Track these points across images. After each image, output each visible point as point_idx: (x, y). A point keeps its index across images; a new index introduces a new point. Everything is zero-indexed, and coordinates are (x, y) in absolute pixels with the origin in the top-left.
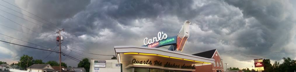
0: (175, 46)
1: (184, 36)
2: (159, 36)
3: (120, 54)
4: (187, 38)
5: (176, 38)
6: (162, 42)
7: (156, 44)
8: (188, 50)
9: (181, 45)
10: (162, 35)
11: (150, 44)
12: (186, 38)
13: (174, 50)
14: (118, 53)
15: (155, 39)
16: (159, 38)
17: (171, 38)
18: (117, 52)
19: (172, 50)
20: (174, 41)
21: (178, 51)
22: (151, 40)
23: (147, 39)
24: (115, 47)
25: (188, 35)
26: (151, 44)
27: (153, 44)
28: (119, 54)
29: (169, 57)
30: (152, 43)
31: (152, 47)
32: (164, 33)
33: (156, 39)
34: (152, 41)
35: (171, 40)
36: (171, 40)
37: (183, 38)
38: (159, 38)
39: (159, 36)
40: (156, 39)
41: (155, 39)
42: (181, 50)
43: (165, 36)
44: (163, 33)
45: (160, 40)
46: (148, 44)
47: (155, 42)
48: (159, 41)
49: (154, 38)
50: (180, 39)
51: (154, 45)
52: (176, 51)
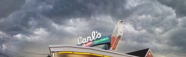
0: (109, 45)
1: (118, 36)
2: (94, 36)
3: (55, 53)
4: (121, 37)
5: (110, 37)
6: (96, 41)
7: (90, 43)
10: (96, 34)
11: (84, 43)
12: (119, 37)
13: (108, 49)
14: (52, 52)
15: (89, 38)
16: (93, 38)
17: (105, 37)
18: (51, 51)
19: (106, 49)
20: (107, 40)
21: (111, 50)
22: (85, 39)
23: (81, 38)
24: (50, 46)
25: (122, 34)
28: (53, 53)
29: (103, 56)
30: (87, 42)
31: (86, 46)
32: (98, 32)
33: (90, 39)
34: (87, 40)
35: (105, 39)
36: (105, 39)
37: (117, 37)
38: (93, 38)
39: (94, 36)
40: (90, 39)
41: (89, 38)
42: (115, 49)
43: (99, 36)
44: (97, 33)
45: (94, 39)
46: (83, 43)
47: (89, 41)
48: (94, 40)
49: (88, 38)
50: (114, 38)
51: (88, 44)
52: (110, 50)
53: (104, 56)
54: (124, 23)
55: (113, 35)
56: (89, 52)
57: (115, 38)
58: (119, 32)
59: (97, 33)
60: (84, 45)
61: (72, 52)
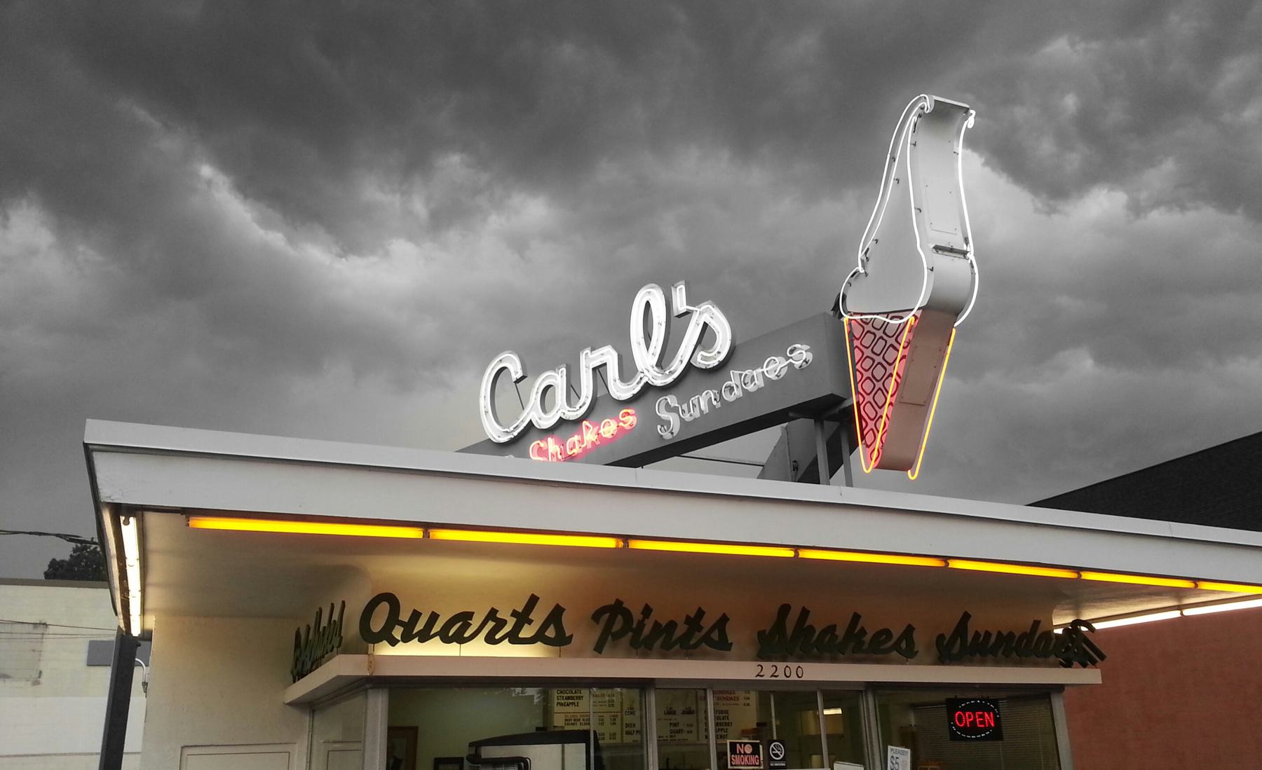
0: (831, 426)
1: (922, 301)
2: (648, 337)
4: (957, 312)
6: (672, 400)
8: (1003, 454)
9: (901, 402)
10: (676, 323)
11: (546, 421)
12: (941, 312)
13: (832, 472)
15: (599, 371)
16: (645, 359)
17: (778, 342)
19: (810, 476)
21: (868, 483)
25: (962, 273)
26: (562, 422)
27: (578, 422)
29: (789, 553)
30: (572, 415)
31: (571, 458)
32: (692, 299)
33: (613, 372)
34: (573, 389)
35: (775, 367)
36: (775, 367)
37: (909, 317)
38: (645, 359)
39: (648, 337)
40: (613, 372)
41: (599, 371)
42: (907, 465)
47: (601, 405)
50: (883, 337)
51: (589, 435)
52: (849, 483)
53: (805, 554)
54: (970, 122)
55: (860, 304)
58: (926, 257)
59: (680, 304)
60: (542, 452)
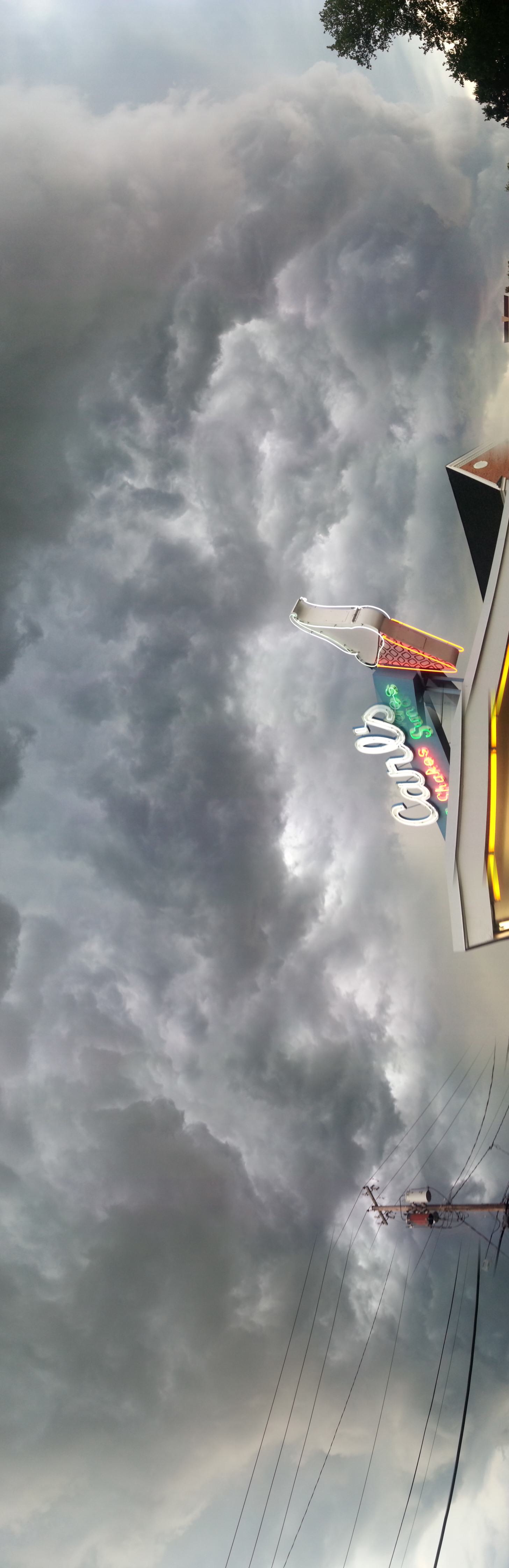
1: (376, 631)
2: (381, 745)
3: (498, 917)
4: (384, 617)
5: (382, 674)
7: (429, 761)
10: (373, 732)
11: (426, 793)
12: (383, 624)
13: (455, 687)
14: (496, 930)
16: (391, 745)
18: (489, 935)
20: (399, 688)
22: (404, 787)
23: (400, 809)
24: (459, 945)
25: (367, 611)
28: (504, 925)
29: (494, 757)
30: (422, 779)
31: (446, 780)
34: (409, 781)
37: (383, 638)
38: (391, 745)
39: (381, 745)
42: (456, 652)
43: (379, 717)
44: (364, 731)
45: (402, 738)
46: (429, 801)
48: (406, 743)
49: (393, 773)
51: (433, 771)
56: (484, 767)
57: (390, 649)
59: (364, 731)
60: (443, 794)
61: (492, 859)
